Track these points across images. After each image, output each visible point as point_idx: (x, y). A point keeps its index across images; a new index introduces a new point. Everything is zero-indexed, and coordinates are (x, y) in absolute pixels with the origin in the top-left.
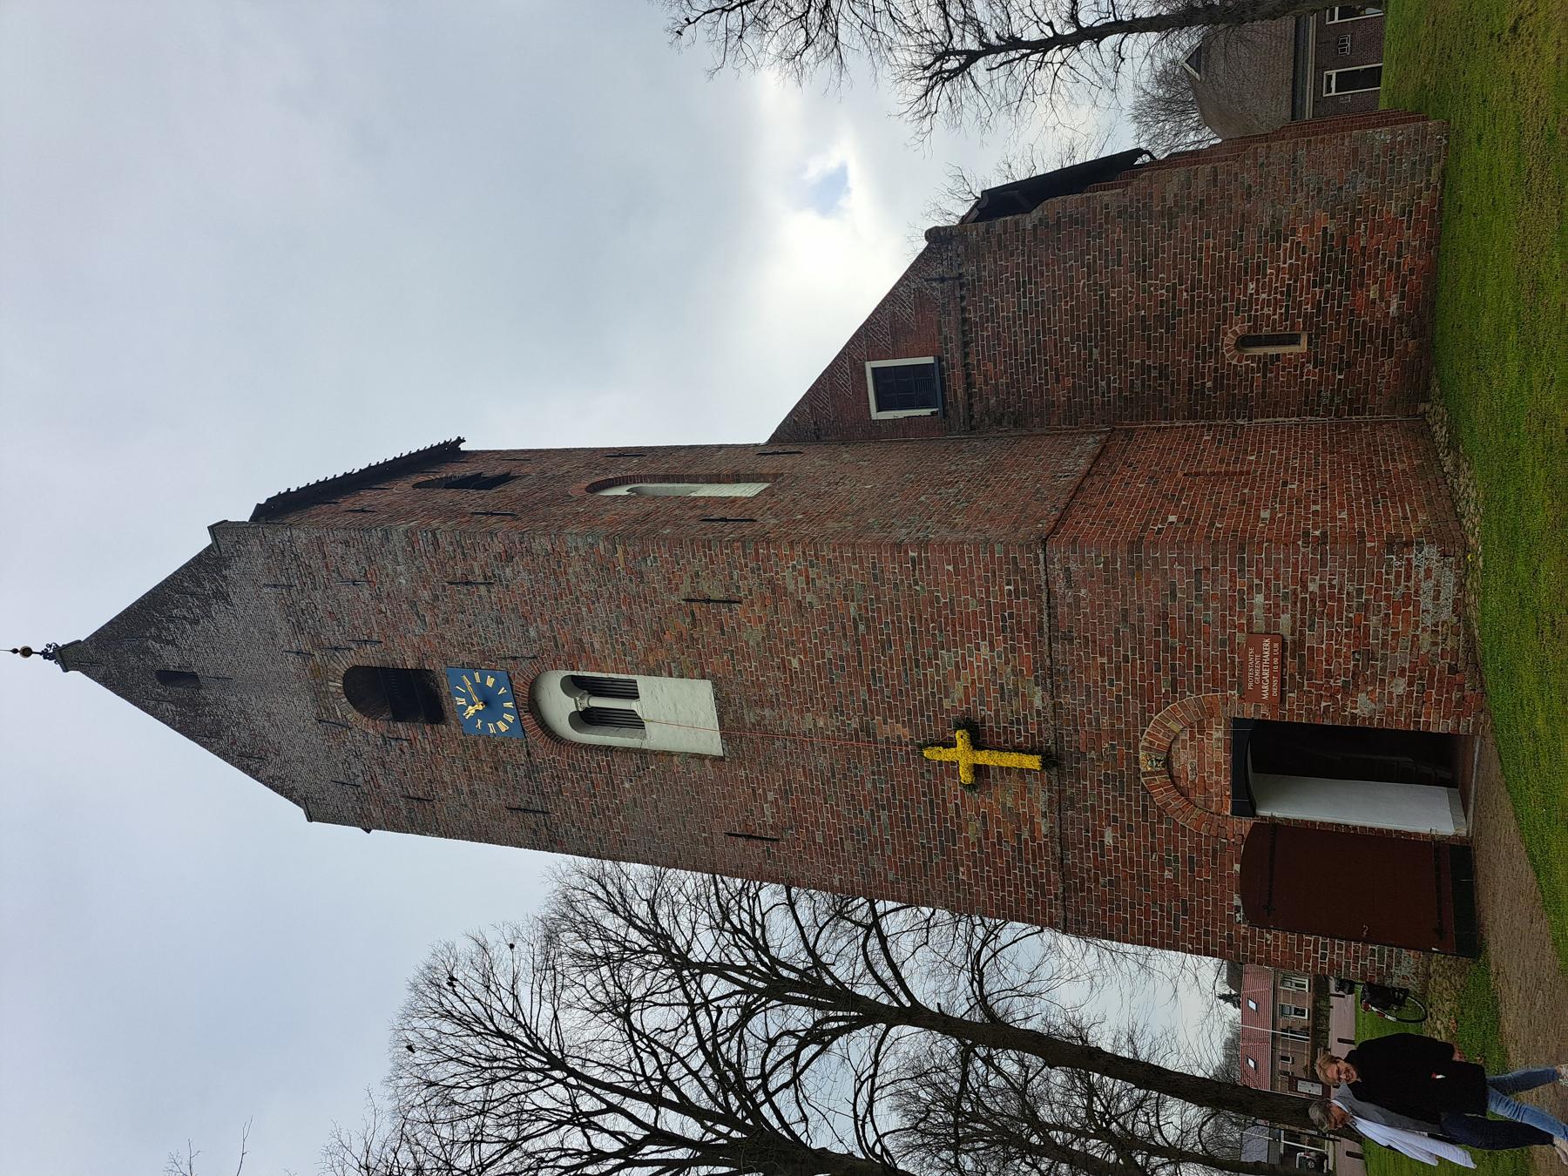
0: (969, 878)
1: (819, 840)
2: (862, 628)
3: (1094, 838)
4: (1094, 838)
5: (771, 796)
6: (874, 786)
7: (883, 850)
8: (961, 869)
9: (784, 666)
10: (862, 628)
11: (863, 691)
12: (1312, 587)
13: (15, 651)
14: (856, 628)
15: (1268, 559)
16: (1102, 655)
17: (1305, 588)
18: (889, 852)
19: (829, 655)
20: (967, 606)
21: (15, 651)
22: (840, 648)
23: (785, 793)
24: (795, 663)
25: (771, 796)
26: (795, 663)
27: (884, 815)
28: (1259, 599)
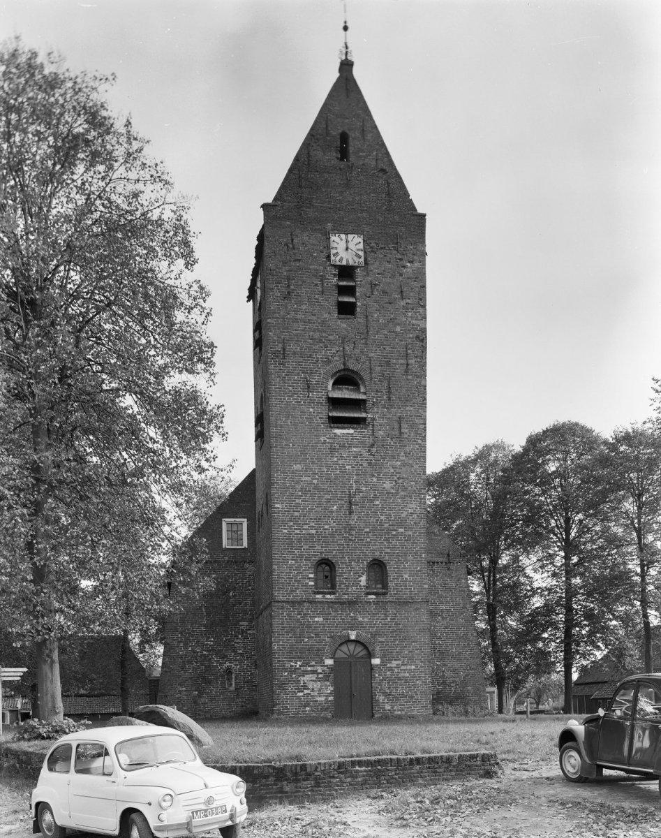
0: (290, 565)
1: (297, 501)
2: (394, 533)
3: (317, 614)
4: (317, 614)
5: (315, 481)
6: (326, 529)
7: (297, 529)
8: (293, 562)
9: (376, 497)
10: (394, 533)
11: (368, 530)
12: (418, 682)
13: (345, 22)
14: (395, 530)
15: (427, 669)
16: (391, 619)
17: (417, 680)
18: (296, 531)
19: (382, 517)
20: (405, 574)
21: (345, 22)
22: (385, 523)
23: (316, 488)
24: (377, 503)
25: (315, 481)
26: (377, 503)
27: (314, 532)
28: (413, 667)
